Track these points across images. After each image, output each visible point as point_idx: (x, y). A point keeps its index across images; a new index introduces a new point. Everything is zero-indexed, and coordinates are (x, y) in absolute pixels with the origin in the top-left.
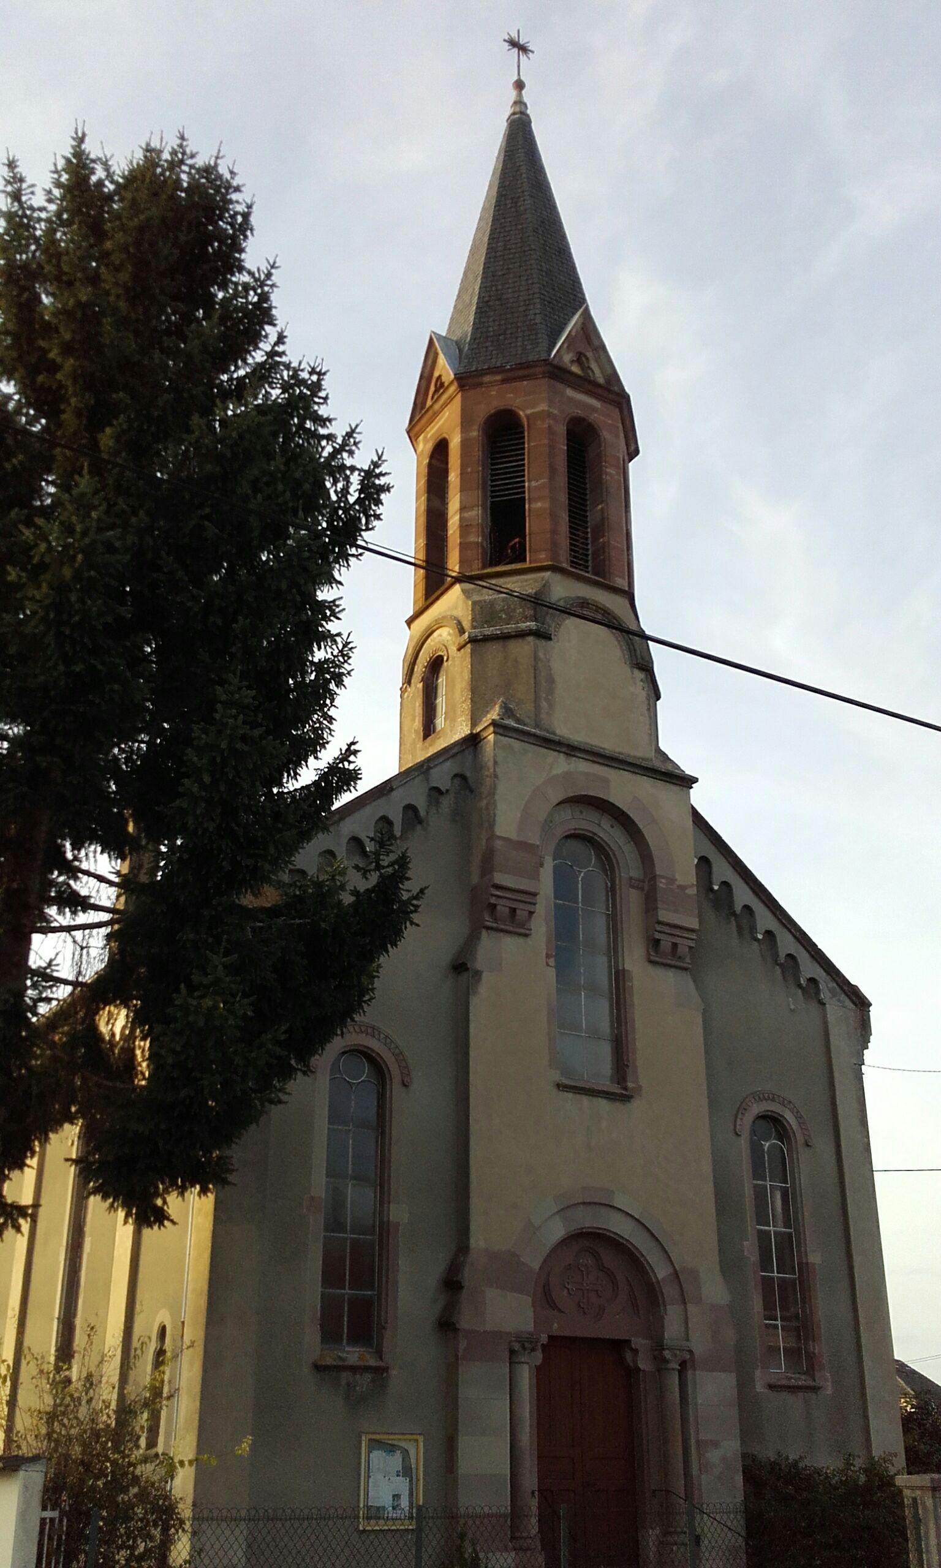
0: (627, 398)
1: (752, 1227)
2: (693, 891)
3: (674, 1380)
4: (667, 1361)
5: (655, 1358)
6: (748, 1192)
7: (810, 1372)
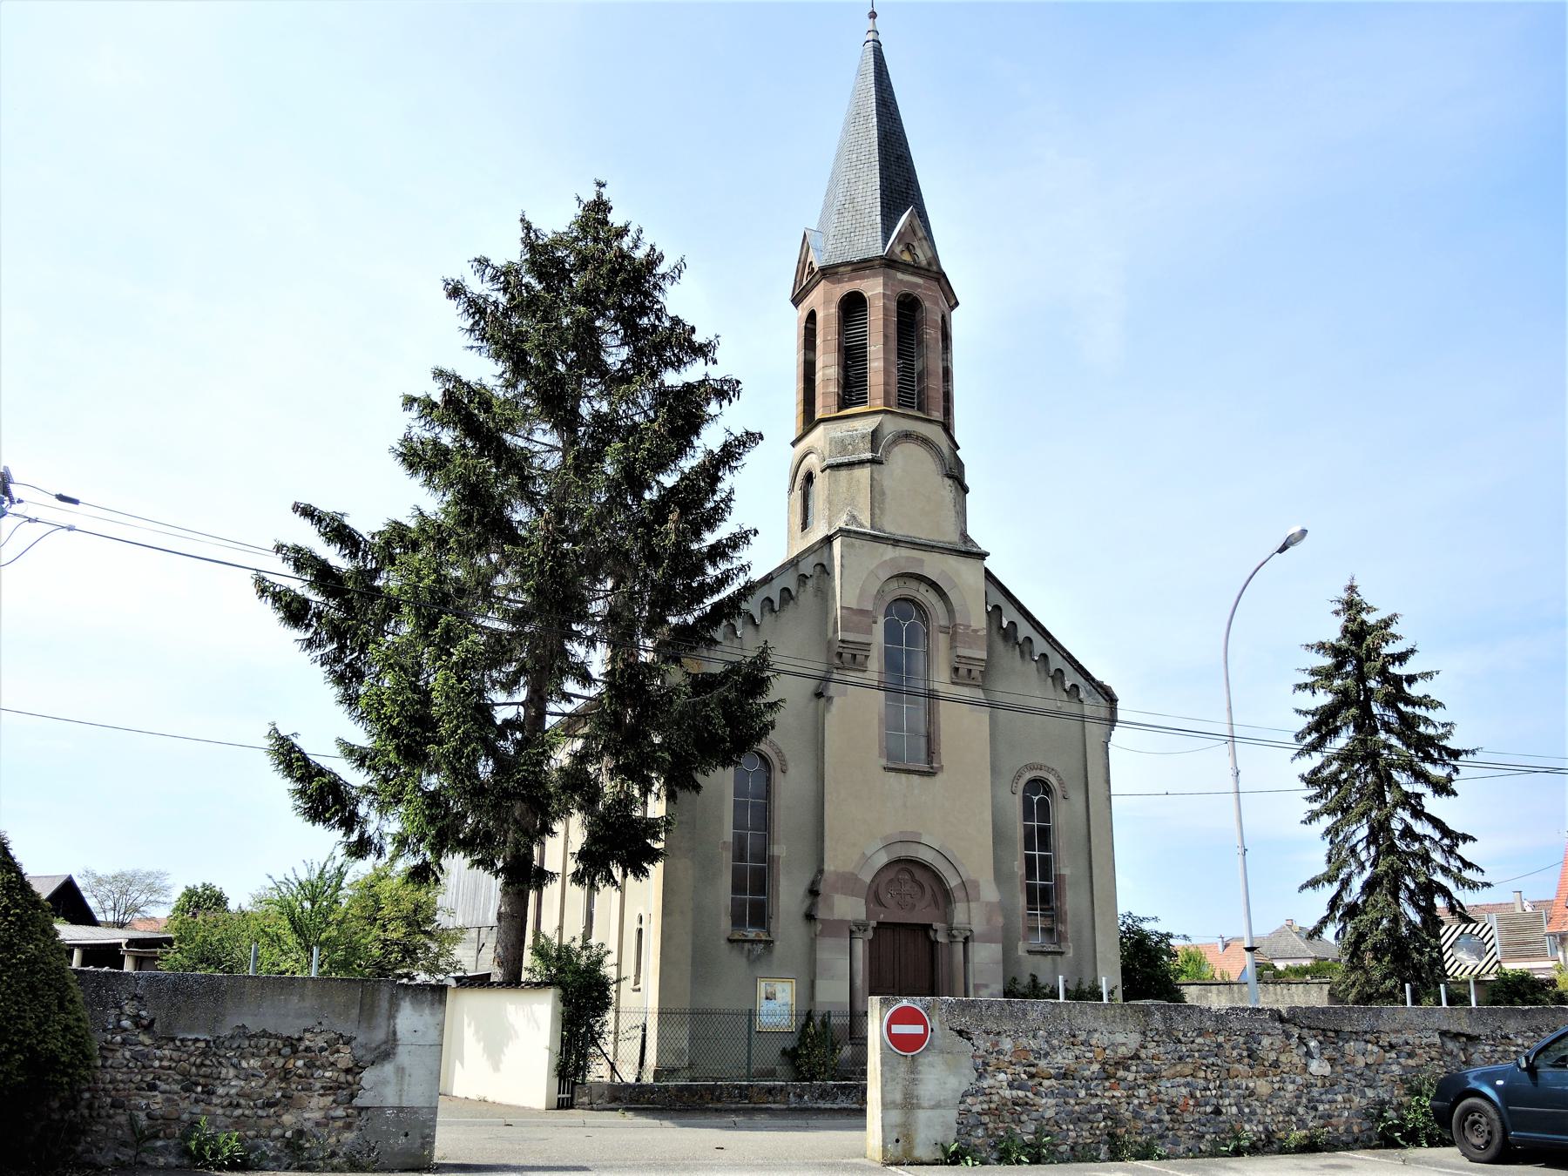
0: (944, 275)
1: (1020, 852)
6: (1020, 834)
7: (1058, 943)
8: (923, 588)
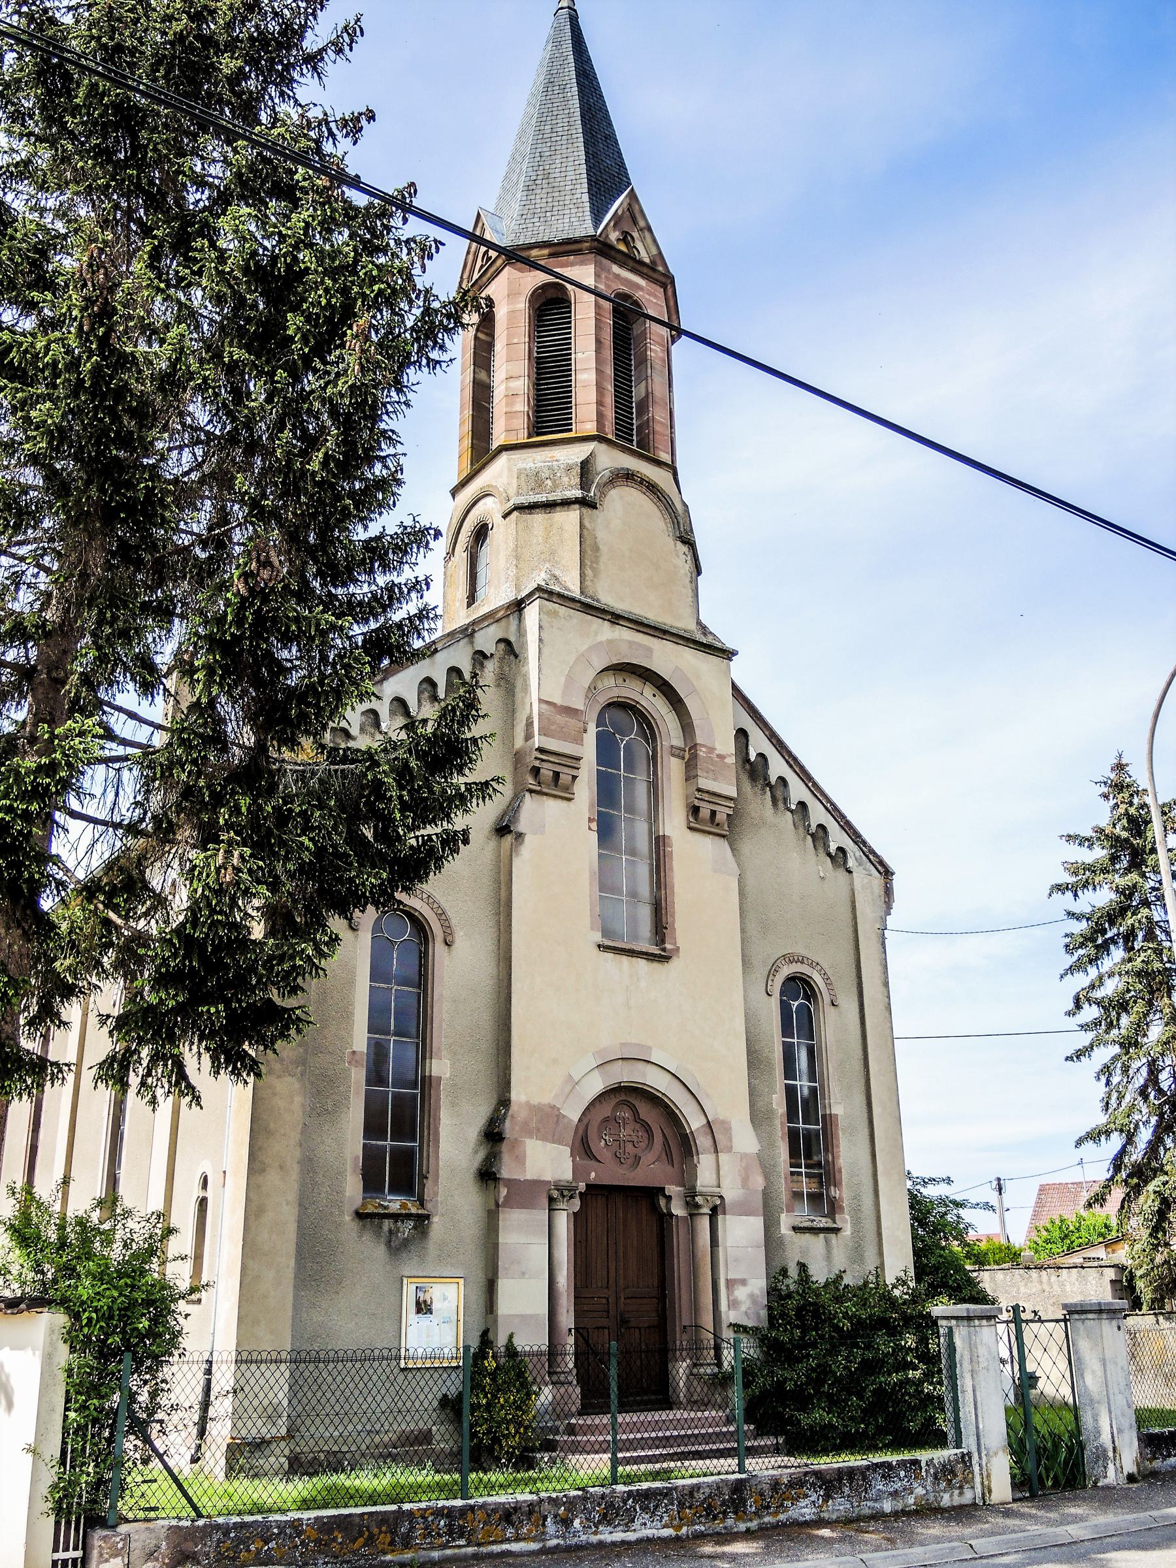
1: (779, 1082)
2: (731, 760)
3: (704, 1224)
4: (698, 1206)
5: (687, 1203)
7: (832, 1215)
8: (649, 691)
